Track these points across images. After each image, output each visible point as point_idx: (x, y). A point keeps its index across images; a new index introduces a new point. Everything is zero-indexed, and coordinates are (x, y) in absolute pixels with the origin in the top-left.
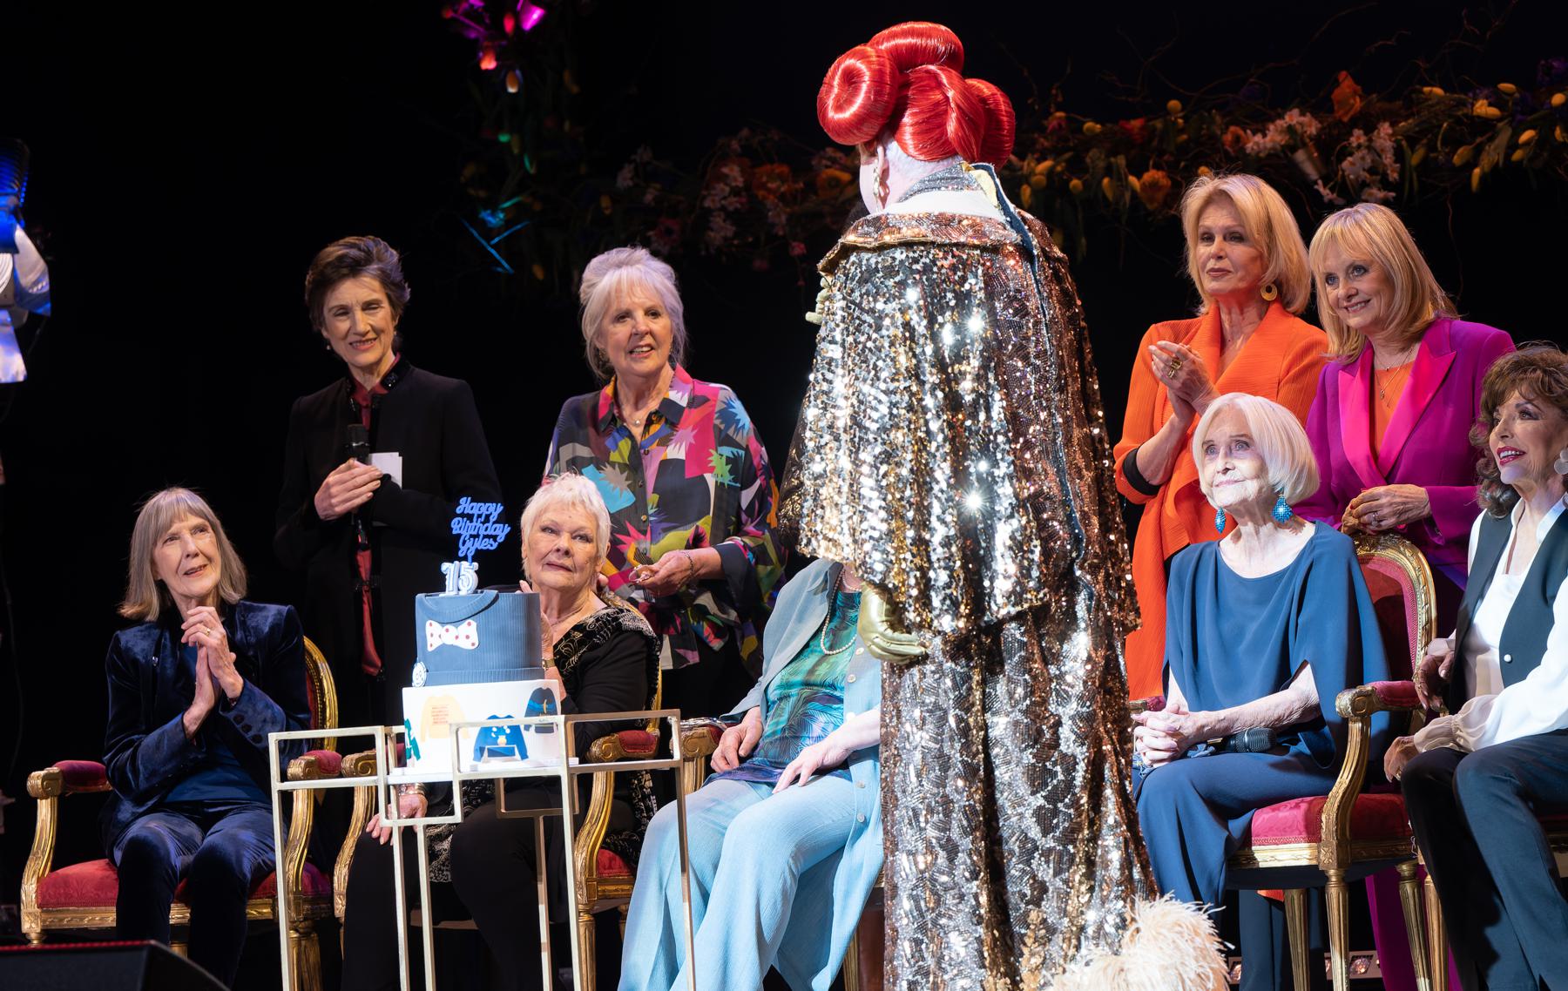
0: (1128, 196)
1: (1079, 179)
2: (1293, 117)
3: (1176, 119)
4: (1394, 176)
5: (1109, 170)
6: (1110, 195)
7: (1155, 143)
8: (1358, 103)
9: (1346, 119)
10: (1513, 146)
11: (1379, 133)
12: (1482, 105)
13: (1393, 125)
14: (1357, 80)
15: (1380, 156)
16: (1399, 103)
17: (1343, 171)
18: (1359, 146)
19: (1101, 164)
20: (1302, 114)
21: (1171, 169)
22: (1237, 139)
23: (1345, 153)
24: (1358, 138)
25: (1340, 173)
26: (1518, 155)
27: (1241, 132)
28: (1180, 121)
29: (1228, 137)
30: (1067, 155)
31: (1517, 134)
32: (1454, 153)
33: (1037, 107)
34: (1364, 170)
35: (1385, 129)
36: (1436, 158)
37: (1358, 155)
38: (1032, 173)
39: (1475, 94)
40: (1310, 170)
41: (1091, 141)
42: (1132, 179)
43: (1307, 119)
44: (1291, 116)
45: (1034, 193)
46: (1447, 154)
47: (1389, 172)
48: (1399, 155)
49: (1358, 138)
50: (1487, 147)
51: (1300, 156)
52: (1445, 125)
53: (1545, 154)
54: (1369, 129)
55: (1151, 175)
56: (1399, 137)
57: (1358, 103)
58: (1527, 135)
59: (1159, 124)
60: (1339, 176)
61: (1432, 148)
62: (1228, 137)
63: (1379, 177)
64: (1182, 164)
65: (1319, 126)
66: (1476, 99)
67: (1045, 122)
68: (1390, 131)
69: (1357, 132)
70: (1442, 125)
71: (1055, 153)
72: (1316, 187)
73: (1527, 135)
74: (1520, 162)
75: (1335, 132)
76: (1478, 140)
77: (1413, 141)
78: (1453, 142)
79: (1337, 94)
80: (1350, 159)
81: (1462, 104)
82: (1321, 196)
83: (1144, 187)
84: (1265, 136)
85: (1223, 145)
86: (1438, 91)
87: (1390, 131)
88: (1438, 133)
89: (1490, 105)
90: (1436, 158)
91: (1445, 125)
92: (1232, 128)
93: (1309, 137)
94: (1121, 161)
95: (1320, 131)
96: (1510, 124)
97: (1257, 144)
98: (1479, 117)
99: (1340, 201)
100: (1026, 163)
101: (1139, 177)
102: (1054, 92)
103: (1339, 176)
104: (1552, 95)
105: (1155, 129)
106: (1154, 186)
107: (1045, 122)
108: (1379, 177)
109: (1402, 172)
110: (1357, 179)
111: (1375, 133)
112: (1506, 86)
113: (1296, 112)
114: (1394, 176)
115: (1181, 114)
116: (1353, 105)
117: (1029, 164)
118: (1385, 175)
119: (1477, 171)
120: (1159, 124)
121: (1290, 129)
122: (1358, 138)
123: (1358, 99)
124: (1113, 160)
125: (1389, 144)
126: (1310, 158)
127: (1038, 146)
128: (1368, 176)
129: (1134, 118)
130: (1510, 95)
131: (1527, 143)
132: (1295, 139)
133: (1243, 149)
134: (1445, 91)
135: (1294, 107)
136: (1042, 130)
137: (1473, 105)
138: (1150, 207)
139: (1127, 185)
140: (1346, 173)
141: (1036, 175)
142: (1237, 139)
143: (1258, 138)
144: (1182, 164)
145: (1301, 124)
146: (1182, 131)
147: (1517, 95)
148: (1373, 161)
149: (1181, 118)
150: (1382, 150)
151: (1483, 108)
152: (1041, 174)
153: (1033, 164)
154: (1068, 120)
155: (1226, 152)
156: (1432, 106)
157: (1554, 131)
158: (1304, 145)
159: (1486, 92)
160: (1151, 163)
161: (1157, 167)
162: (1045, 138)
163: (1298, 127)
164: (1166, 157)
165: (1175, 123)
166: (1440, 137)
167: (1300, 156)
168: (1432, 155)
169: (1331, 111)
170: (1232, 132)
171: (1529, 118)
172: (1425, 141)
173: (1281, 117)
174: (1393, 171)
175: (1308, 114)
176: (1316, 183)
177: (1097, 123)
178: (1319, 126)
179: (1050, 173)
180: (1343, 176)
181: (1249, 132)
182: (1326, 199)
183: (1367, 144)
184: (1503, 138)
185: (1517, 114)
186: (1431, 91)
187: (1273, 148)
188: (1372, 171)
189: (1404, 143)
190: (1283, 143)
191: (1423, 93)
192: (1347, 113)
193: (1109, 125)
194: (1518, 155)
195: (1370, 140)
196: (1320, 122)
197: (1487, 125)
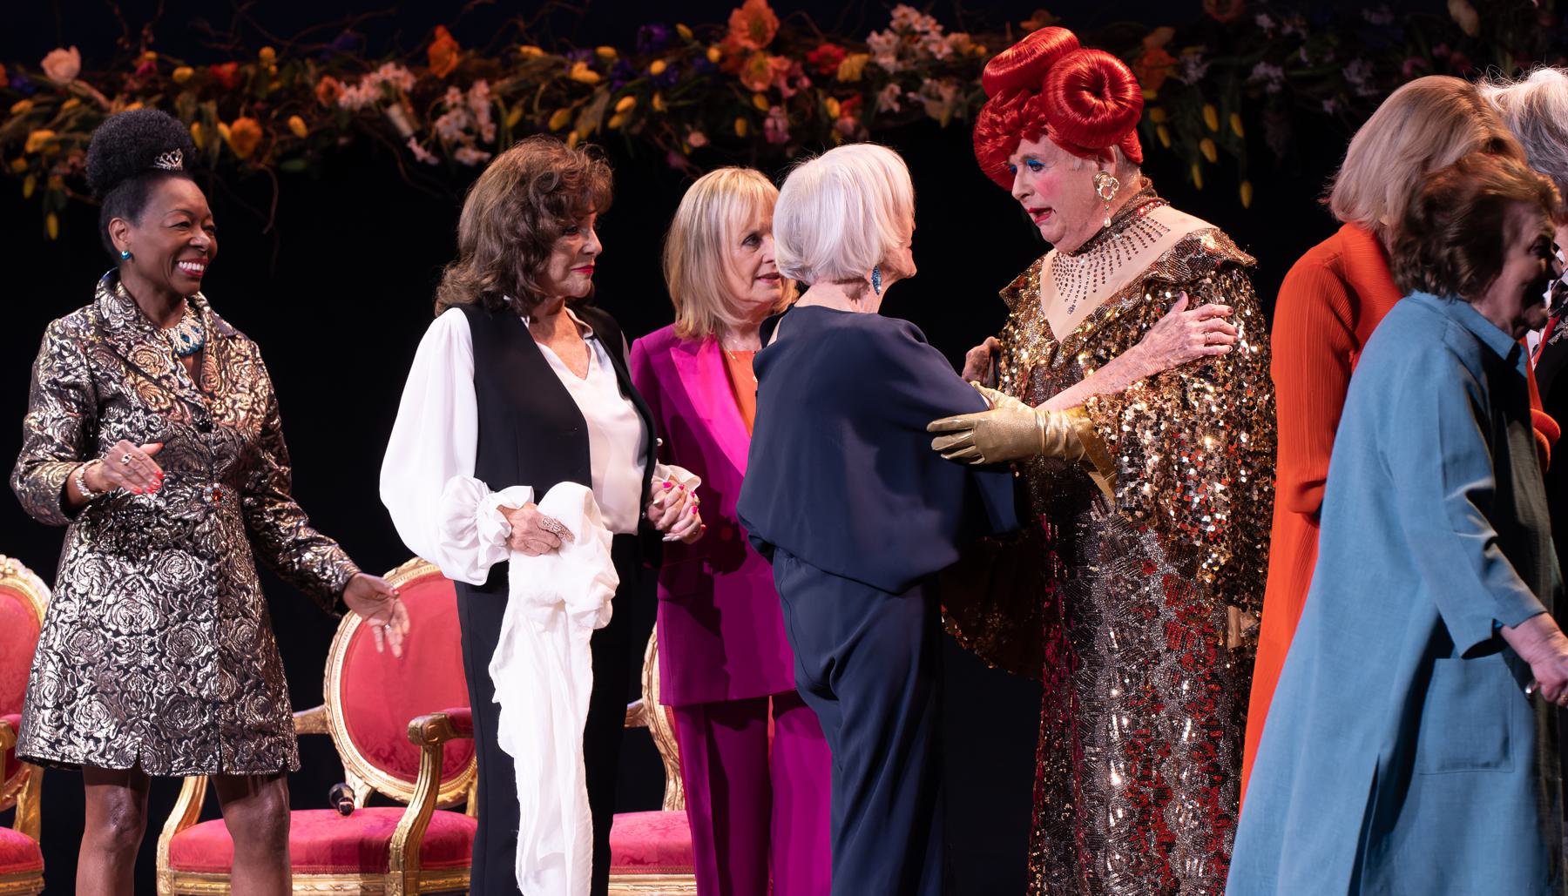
0: (217, 145)
3: (269, 65)
4: (489, 137)
5: (199, 116)
6: (199, 142)
7: (247, 90)
8: (455, 60)
9: (442, 75)
10: (610, 112)
11: (475, 96)
12: (581, 69)
13: (490, 84)
14: (455, 35)
16: (496, 62)
17: (437, 130)
18: (454, 106)
19: (191, 110)
20: (398, 67)
21: (262, 118)
22: (330, 90)
23: (440, 111)
24: (453, 95)
25: (434, 132)
26: (615, 122)
28: (273, 69)
29: (321, 89)
31: (615, 98)
32: (551, 115)
33: (127, 46)
35: (481, 88)
36: (532, 121)
37: (454, 114)
39: (574, 55)
41: (177, 88)
42: (223, 129)
43: (402, 73)
44: (386, 73)
46: (543, 118)
47: (484, 132)
48: (495, 115)
49: (454, 96)
50: (584, 112)
51: (395, 112)
52: (543, 87)
53: (643, 121)
54: (465, 87)
55: (243, 123)
56: (496, 97)
57: (455, 60)
58: (625, 103)
59: (251, 70)
60: (433, 136)
61: (528, 109)
62: (321, 89)
63: (472, 138)
64: (274, 113)
66: (574, 61)
67: (135, 63)
70: (537, 87)
71: (145, 94)
73: (625, 103)
74: (617, 129)
75: (430, 87)
76: (576, 103)
77: (509, 102)
78: (551, 105)
80: (444, 118)
81: (560, 66)
82: (411, 154)
83: (233, 135)
84: (358, 88)
85: (316, 95)
86: (536, 52)
88: (533, 97)
89: (590, 68)
90: (532, 121)
91: (543, 87)
92: (327, 80)
93: (406, 93)
94: (211, 107)
95: (415, 86)
96: (609, 88)
97: (351, 97)
98: (577, 82)
99: (486, 156)
100: (114, 105)
101: (229, 123)
102: (145, 32)
103: (433, 136)
104: (651, 61)
105: (246, 75)
106: (243, 136)
107: (135, 63)
108: (472, 138)
109: (497, 134)
110: (450, 140)
111: (471, 93)
112: (606, 51)
114: (489, 137)
116: (449, 62)
117: (117, 106)
118: (479, 136)
120: (251, 70)
121: (385, 84)
122: (454, 96)
124: (203, 106)
126: (404, 113)
127: (127, 87)
129: (227, 61)
130: (611, 59)
131: (625, 111)
132: (389, 95)
133: (335, 102)
134: (544, 49)
135: (392, 60)
136: (133, 70)
137: (571, 68)
138: (241, 155)
139: (217, 134)
142: (331, 91)
143: (352, 91)
144: (274, 113)
145: (397, 78)
146: (275, 78)
147: (617, 60)
148: (469, 121)
150: (479, 110)
151: (581, 72)
153: (121, 107)
154: (160, 61)
155: (319, 105)
156: (527, 68)
157: (651, 98)
158: (398, 100)
159: (585, 54)
160: (242, 110)
161: (248, 115)
162: (135, 79)
163: (394, 83)
164: (259, 105)
165: (267, 70)
166: (537, 98)
168: (529, 117)
169: (427, 64)
170: (327, 84)
171: (629, 84)
172: (522, 102)
173: (375, 69)
174: (489, 131)
176: (408, 139)
177: (188, 65)
180: (438, 137)
181: (343, 85)
185: (618, 79)
186: (529, 53)
187: (367, 102)
188: (467, 131)
189: (501, 104)
191: (518, 51)
192: (443, 69)
193: (201, 68)
194: (615, 122)
195: (465, 99)
196: (416, 75)
197: (585, 90)
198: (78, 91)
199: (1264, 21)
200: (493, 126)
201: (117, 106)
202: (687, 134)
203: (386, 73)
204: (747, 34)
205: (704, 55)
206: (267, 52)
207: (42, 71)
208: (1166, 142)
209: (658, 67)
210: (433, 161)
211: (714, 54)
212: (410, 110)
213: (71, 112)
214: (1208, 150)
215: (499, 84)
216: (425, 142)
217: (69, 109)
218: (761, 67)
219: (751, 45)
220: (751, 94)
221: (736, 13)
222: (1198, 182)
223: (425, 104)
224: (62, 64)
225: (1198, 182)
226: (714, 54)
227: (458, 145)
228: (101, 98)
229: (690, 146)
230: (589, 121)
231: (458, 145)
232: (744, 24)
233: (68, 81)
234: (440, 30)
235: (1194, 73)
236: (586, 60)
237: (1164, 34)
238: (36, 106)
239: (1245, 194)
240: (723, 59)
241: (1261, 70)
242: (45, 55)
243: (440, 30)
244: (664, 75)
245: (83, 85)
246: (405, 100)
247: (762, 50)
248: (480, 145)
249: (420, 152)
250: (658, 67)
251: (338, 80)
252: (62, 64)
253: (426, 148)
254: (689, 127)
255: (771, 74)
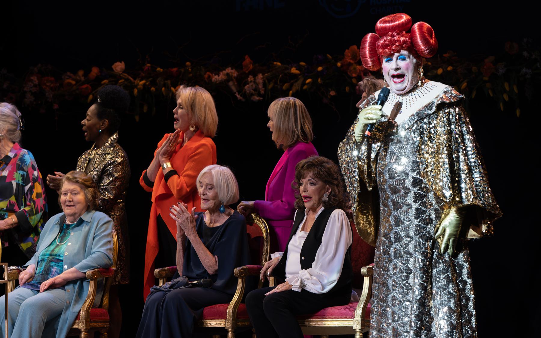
0: (170, 94)
1: (154, 87)
2: (229, 70)
3: (189, 68)
4: (262, 92)
5: (164, 85)
6: (164, 94)
8: (251, 66)
9: (247, 72)
10: (304, 84)
11: (258, 77)
12: (293, 70)
13: (263, 75)
15: (258, 85)
17: (245, 89)
18: (251, 81)
19: (162, 83)
20: (232, 69)
23: (247, 83)
24: (250, 78)
25: (244, 90)
26: (305, 87)
27: (210, 74)
28: (190, 69)
29: (206, 76)
30: (151, 79)
32: (284, 85)
33: (141, 62)
34: (252, 89)
35: (260, 76)
37: (251, 84)
38: (138, 84)
40: (234, 88)
42: (172, 89)
43: (233, 71)
44: (228, 71)
45: (138, 91)
47: (261, 91)
48: (264, 85)
49: (251, 78)
50: (295, 84)
51: (231, 84)
52: (281, 76)
54: (255, 76)
56: (265, 79)
57: (251, 66)
58: (309, 81)
59: (182, 70)
62: (206, 76)
63: (257, 92)
65: (238, 73)
66: (292, 67)
68: (262, 77)
69: (251, 76)
70: (279, 76)
72: (236, 95)
73: (309, 81)
76: (292, 81)
79: (244, 63)
80: (248, 85)
84: (219, 76)
86: (279, 64)
87: (262, 77)
89: (297, 69)
91: (281, 76)
92: (208, 73)
93: (234, 77)
94: (169, 82)
97: (216, 79)
98: (293, 73)
100: (136, 81)
102: (147, 57)
104: (318, 67)
108: (257, 92)
109: (265, 92)
111: (257, 77)
112: (302, 63)
113: (230, 68)
114: (262, 92)
115: (190, 67)
116: (249, 67)
117: (137, 81)
118: (259, 92)
119: (291, 92)
120: (182, 70)
121: (228, 74)
122: (251, 78)
123: (251, 65)
124: (166, 82)
125: (261, 81)
128: (253, 91)
131: (309, 83)
133: (211, 80)
134: (282, 64)
137: (291, 69)
139: (171, 91)
140: (246, 90)
141: (139, 85)
143: (216, 77)
148: (256, 87)
149: (190, 68)
150: (259, 83)
151: (294, 70)
152: (141, 85)
153: (138, 82)
157: (318, 80)
158: (232, 80)
163: (230, 74)
167: (231, 84)
168: (276, 86)
172: (273, 81)
173: (225, 70)
175: (234, 70)
176: (235, 93)
177: (161, 68)
178: (238, 73)
179: (144, 85)
180: (245, 92)
181: (213, 74)
182: (239, 99)
183: (254, 81)
184: (300, 82)
186: (276, 64)
188: (255, 90)
189: (266, 81)
190: (225, 79)
191: (273, 64)
194: (305, 87)
195: (255, 79)
196: (238, 73)
197: (295, 76)
198: (124, 77)
199: (525, 54)
200: (264, 89)
201: (137, 81)
202: (330, 92)
203: (228, 71)
204: (350, 58)
205: (336, 65)
206: (188, 63)
207: (112, 70)
208: (491, 95)
209: (320, 69)
210: (243, 100)
211: (339, 64)
212: (236, 83)
213: (121, 84)
214: (506, 97)
215: (266, 75)
216: (241, 94)
217: (120, 83)
218: (355, 69)
219: (352, 61)
220: (351, 78)
221: (347, 51)
222: (502, 109)
223: (241, 81)
224: (119, 67)
225: (502, 109)
226: (339, 64)
227: (252, 95)
228: (132, 79)
229: (330, 95)
230: (296, 87)
231: (252, 95)
232: (350, 54)
233: (121, 73)
234: (247, 56)
235: (501, 71)
236: (295, 67)
237: (492, 58)
238: (109, 82)
239: (518, 112)
240: (342, 66)
241: (524, 70)
242: (113, 64)
243: (247, 56)
244: (322, 71)
245: (126, 75)
246: (234, 80)
247: (355, 63)
248: (259, 95)
249: (238, 96)
250: (320, 69)
251: (212, 74)
252: (119, 67)
253: (241, 96)
254: (330, 89)
255: (358, 71)
